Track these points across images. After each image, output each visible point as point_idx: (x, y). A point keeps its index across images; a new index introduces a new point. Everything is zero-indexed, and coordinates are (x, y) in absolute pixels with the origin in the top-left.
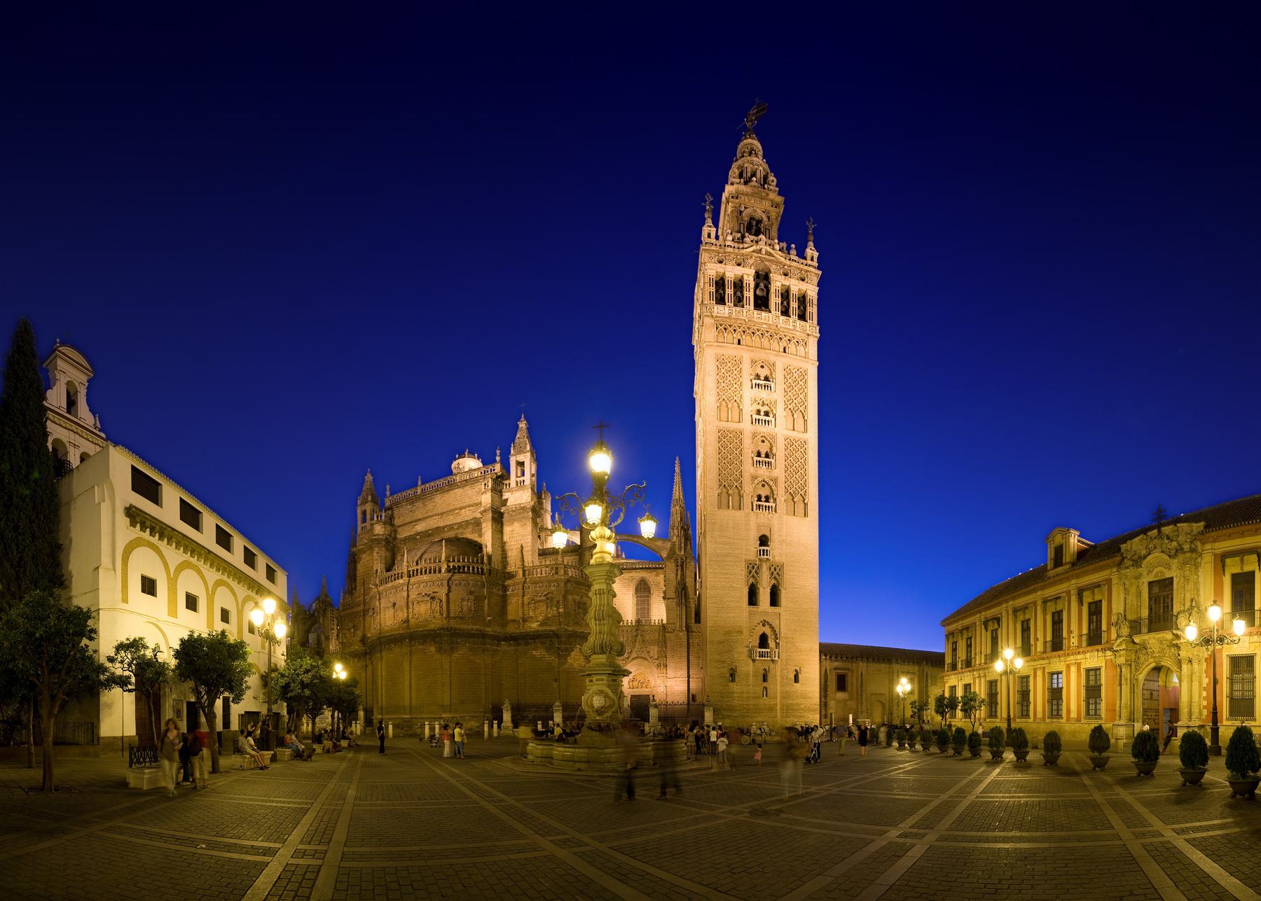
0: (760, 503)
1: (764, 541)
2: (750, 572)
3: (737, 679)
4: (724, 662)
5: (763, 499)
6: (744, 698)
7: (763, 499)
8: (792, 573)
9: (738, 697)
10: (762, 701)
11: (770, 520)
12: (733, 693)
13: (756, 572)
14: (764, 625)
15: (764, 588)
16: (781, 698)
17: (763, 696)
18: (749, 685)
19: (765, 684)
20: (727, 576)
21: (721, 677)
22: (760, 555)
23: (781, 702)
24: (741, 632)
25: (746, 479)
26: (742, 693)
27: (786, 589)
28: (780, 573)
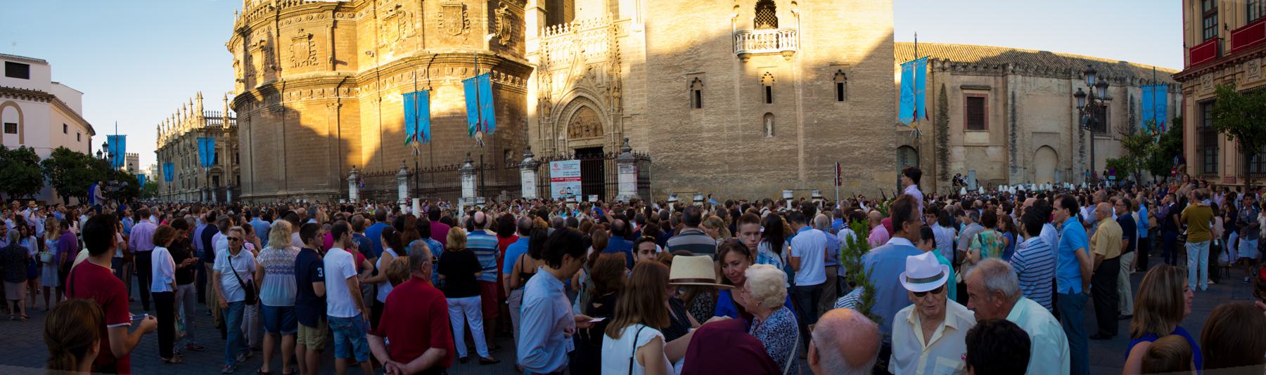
3: (706, 100)
6: (724, 140)
9: (710, 139)
10: (763, 145)
12: (700, 130)
16: (806, 136)
18: (733, 112)
19: (769, 108)
21: (675, 99)
23: (805, 147)
26: (718, 129)
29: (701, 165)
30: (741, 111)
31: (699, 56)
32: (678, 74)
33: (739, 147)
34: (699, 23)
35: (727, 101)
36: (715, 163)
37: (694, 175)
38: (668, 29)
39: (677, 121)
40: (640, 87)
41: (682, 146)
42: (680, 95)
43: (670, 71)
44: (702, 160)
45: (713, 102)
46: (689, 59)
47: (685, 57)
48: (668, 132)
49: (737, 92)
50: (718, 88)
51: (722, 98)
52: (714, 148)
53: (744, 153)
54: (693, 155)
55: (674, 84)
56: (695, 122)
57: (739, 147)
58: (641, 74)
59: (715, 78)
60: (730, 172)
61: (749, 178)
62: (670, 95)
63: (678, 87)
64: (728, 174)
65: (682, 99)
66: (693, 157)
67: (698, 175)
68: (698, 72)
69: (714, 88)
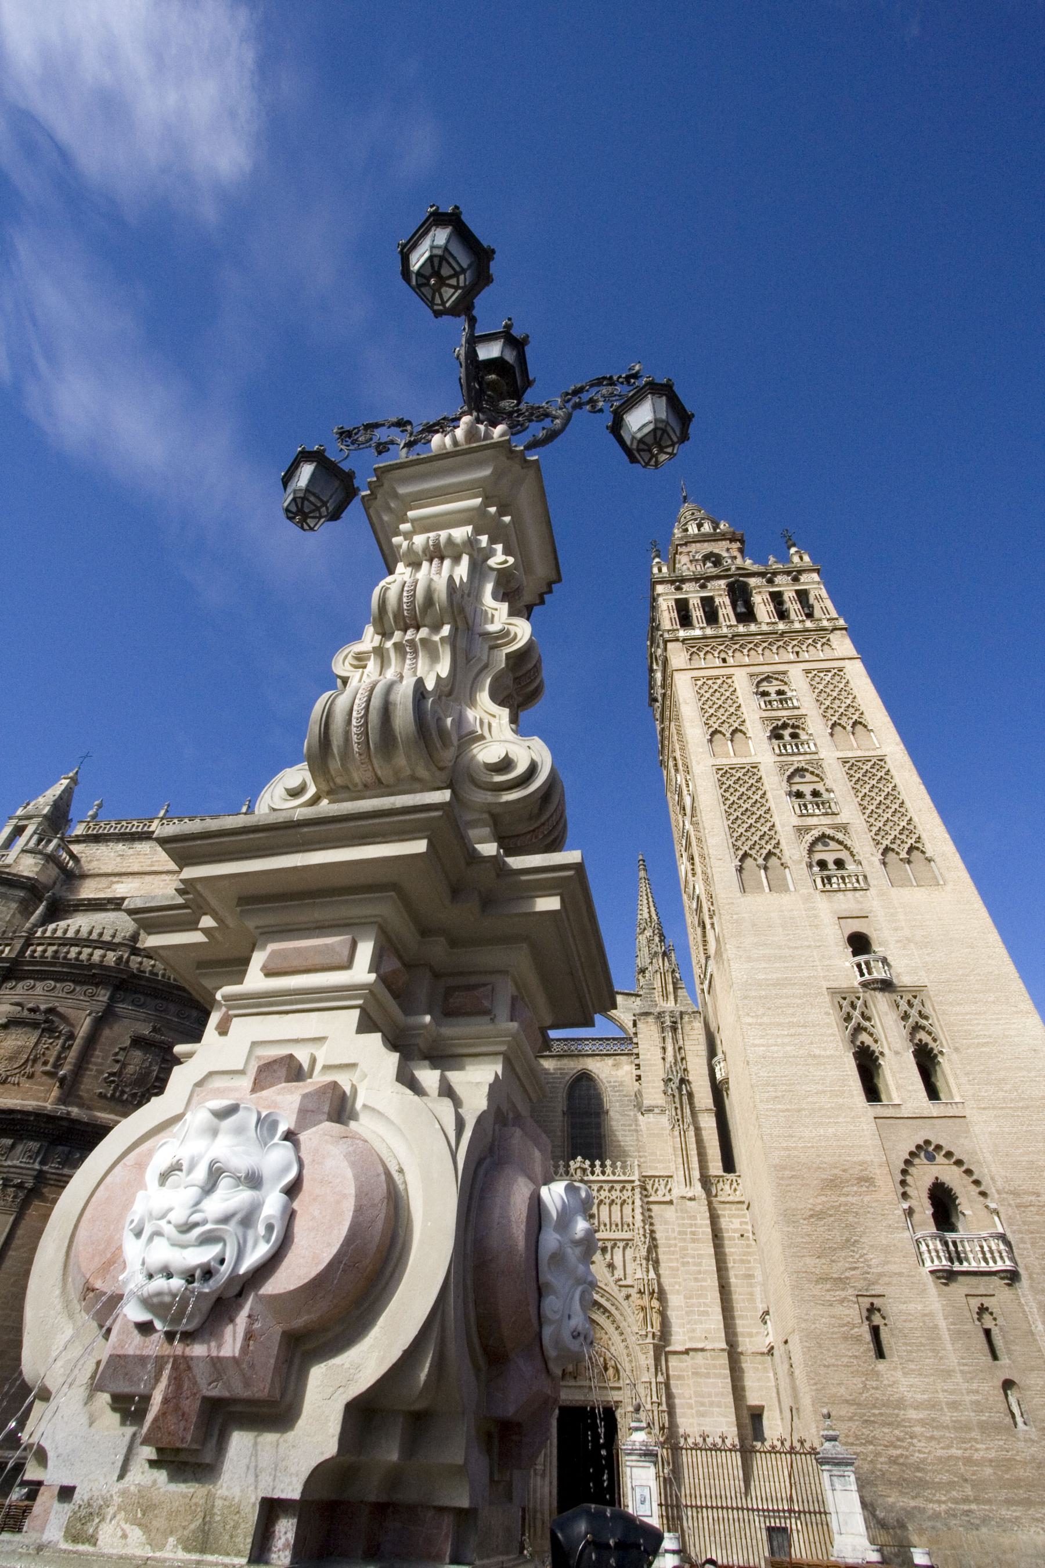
0: (826, 873)
1: (859, 943)
2: (848, 1018)
4: (841, 1282)
5: (831, 866)
6: (947, 1427)
7: (831, 866)
8: (957, 1009)
9: (922, 1423)
11: (861, 903)
12: (900, 1404)
13: (863, 1014)
14: (931, 1158)
15: (897, 1053)
17: (1016, 1424)
20: (792, 1031)
21: (845, 1338)
22: (862, 975)
24: (867, 1181)
25: (785, 834)
26: (933, 1405)
27: (956, 1050)
28: (928, 1010)
29: (920, 1479)
30: (962, 1372)
31: (869, 1266)
32: (843, 1294)
33: (978, 1446)
34: (857, 1213)
35: (933, 1350)
36: (945, 1477)
37: (913, 1503)
38: (811, 1216)
39: (857, 1382)
40: (699, 1296)
41: (877, 1433)
42: (852, 1332)
43: (828, 1286)
44: (919, 1469)
45: (911, 1352)
46: (855, 1269)
47: (847, 1265)
48: (847, 1401)
49: (946, 1336)
50: (911, 1325)
51: (924, 1345)
52: (933, 1443)
53: (991, 1461)
54: (902, 1455)
55: (839, 1310)
56: (889, 1386)
57: (978, 1446)
58: (699, 1272)
59: (903, 1307)
60: (976, 1500)
61: (1017, 1518)
62: (836, 1330)
63: (847, 1315)
64: (974, 1507)
65: (858, 1339)
66: (901, 1460)
67: (919, 1503)
68: (873, 1293)
69: (908, 1325)
